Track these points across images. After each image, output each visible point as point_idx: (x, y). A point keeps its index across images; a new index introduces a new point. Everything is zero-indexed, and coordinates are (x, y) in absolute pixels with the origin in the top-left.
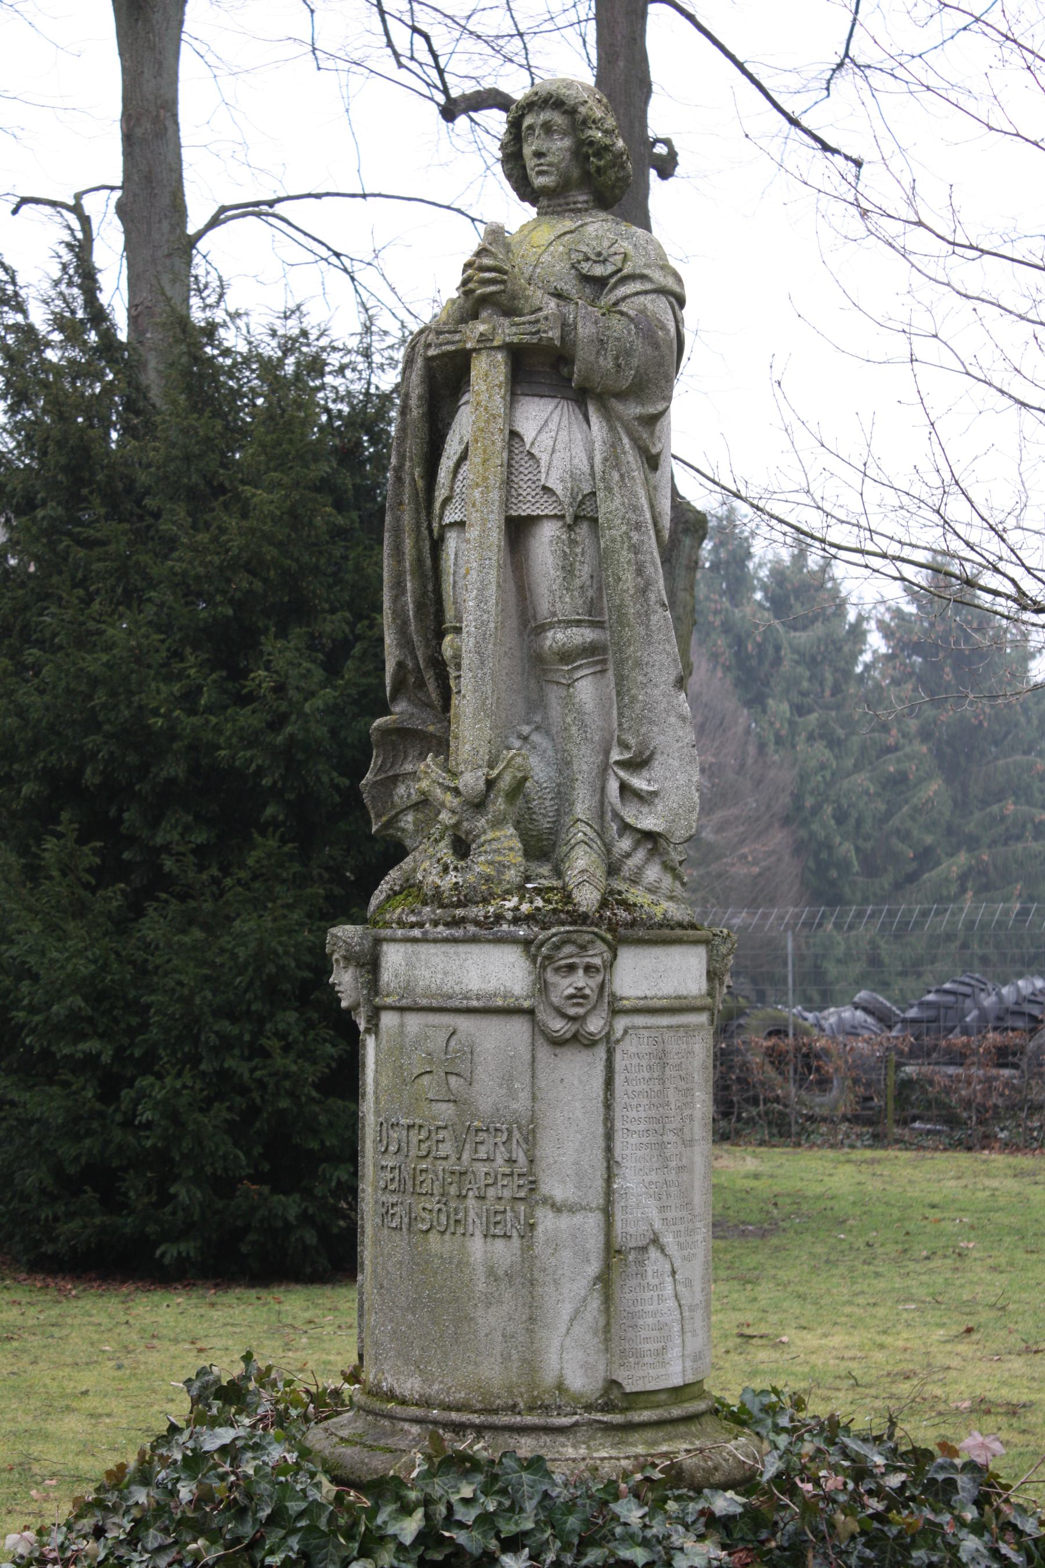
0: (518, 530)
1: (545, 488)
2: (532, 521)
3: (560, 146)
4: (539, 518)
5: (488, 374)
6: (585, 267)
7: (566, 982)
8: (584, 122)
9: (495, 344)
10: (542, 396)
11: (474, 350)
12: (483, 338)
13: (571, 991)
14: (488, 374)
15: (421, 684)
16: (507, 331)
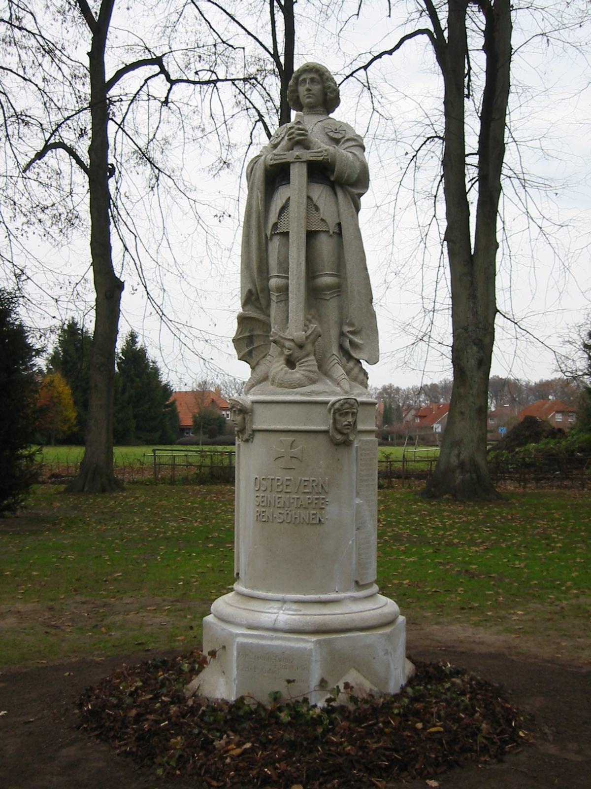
0: (311, 235)
1: (322, 220)
2: (317, 232)
3: (316, 88)
4: (319, 231)
5: (298, 174)
6: (331, 134)
7: (343, 419)
8: (327, 79)
9: (303, 160)
10: (318, 183)
11: (293, 162)
12: (298, 157)
13: (346, 423)
14: (298, 174)
15: (258, 299)
16: (307, 155)
